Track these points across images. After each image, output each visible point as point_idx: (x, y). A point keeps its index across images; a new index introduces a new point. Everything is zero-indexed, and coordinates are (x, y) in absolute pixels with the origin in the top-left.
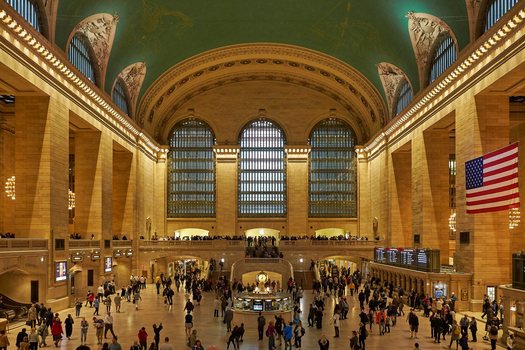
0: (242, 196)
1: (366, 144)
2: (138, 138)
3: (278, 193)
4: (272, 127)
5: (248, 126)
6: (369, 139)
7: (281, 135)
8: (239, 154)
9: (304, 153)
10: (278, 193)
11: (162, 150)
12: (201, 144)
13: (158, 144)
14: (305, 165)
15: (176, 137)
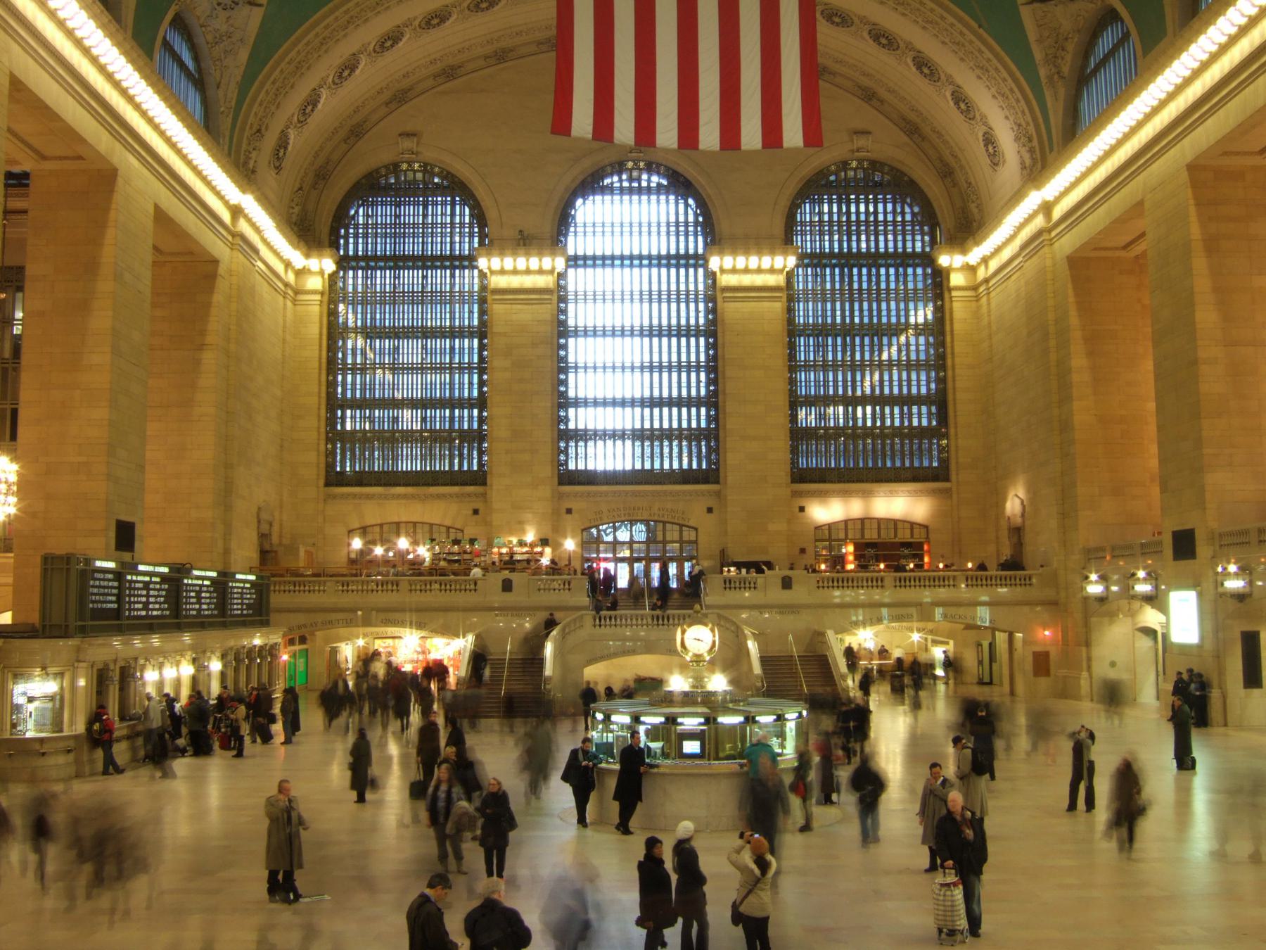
0: (571, 411)
1: (970, 242)
2: (236, 211)
3: (689, 402)
4: (666, 190)
5: (590, 184)
6: (979, 228)
7: (696, 215)
8: (562, 276)
9: (772, 271)
10: (689, 402)
11: (314, 263)
12: (436, 247)
13: (302, 244)
14: (777, 307)
15: (356, 227)
